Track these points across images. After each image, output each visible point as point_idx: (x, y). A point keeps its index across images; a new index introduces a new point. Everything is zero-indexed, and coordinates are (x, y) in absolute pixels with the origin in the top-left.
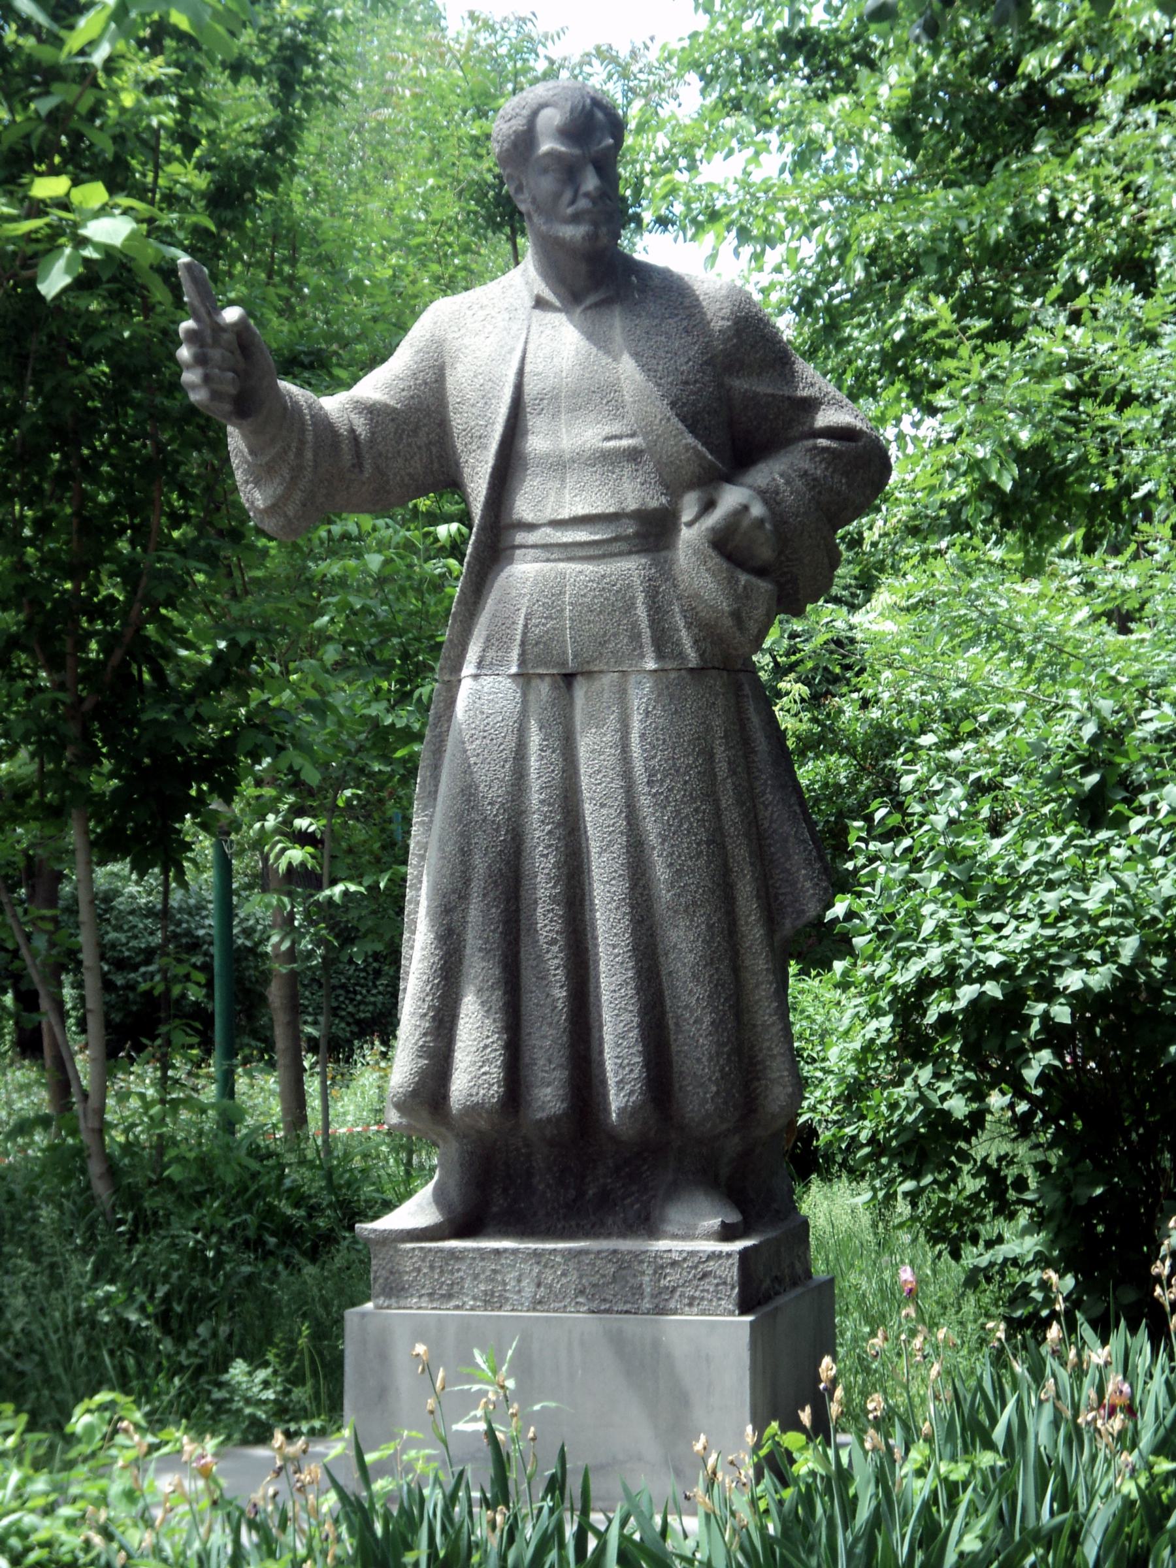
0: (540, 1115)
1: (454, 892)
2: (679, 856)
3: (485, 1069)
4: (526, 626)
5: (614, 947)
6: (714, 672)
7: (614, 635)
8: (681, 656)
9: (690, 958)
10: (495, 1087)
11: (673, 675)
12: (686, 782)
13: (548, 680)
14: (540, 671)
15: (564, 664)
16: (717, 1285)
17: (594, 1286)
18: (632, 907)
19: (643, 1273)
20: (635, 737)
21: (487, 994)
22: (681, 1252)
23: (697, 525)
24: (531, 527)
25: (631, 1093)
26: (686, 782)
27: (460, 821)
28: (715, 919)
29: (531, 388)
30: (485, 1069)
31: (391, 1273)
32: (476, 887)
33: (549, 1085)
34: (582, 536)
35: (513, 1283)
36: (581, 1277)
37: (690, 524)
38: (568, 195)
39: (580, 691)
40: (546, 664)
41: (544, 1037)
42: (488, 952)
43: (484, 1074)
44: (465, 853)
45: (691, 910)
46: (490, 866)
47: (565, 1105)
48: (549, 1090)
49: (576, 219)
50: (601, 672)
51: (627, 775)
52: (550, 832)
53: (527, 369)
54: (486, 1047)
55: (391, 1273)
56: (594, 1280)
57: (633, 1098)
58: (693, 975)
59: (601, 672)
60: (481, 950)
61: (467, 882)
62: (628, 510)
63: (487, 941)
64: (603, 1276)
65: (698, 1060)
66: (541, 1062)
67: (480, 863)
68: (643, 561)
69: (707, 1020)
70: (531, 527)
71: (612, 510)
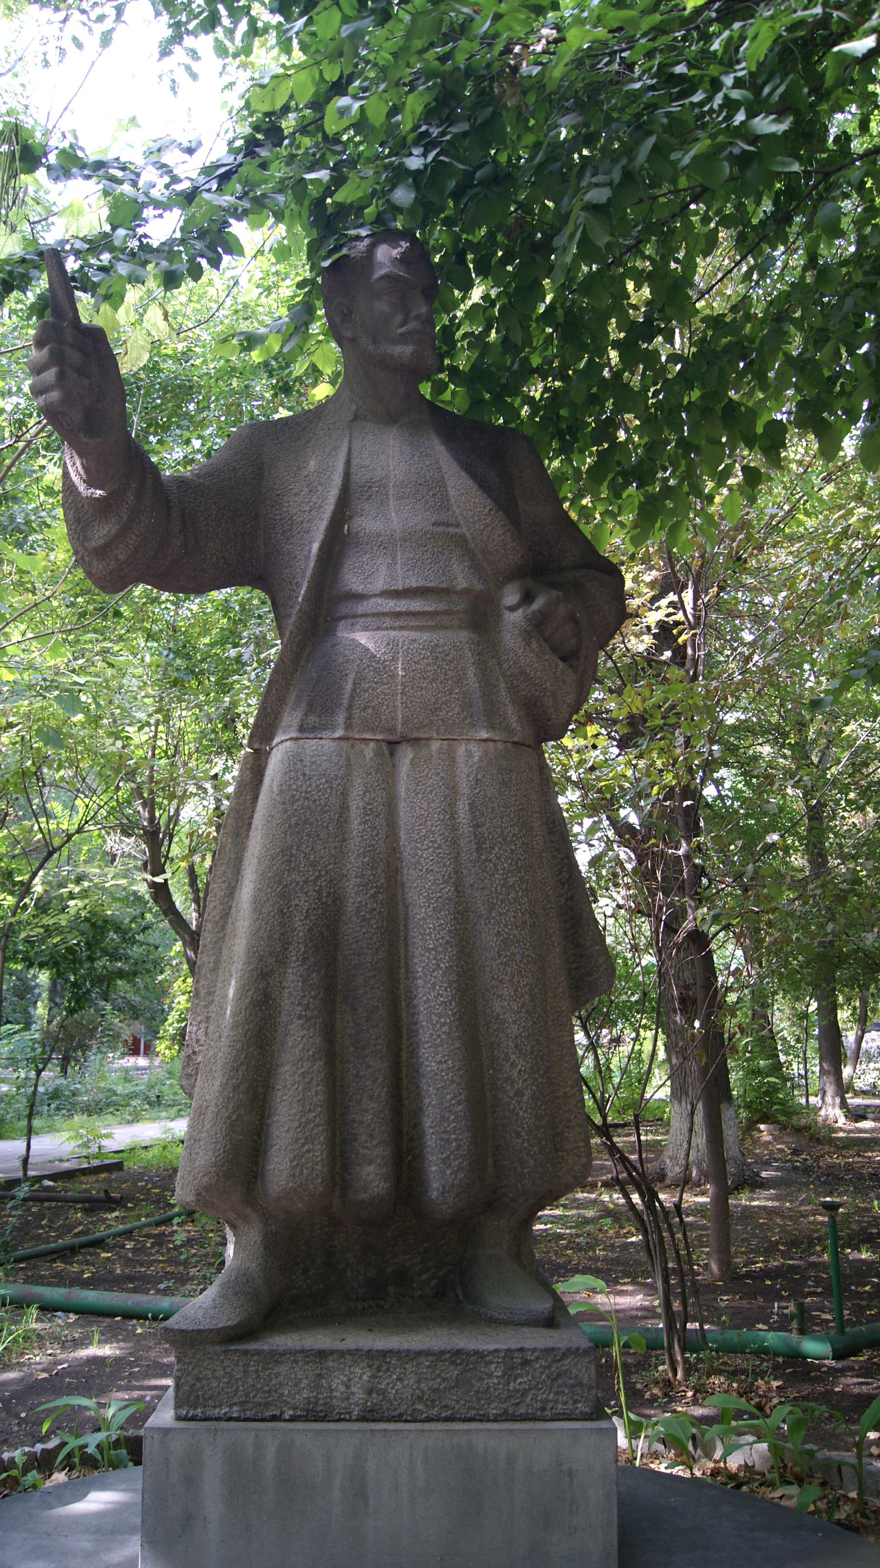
0: (363, 1196)
1: (271, 954)
2: (506, 926)
3: (306, 1148)
4: (354, 690)
5: (440, 1016)
6: (530, 750)
7: (446, 703)
8: (507, 729)
9: (514, 1029)
10: (319, 1167)
11: (500, 745)
12: (512, 851)
13: (372, 745)
14: (367, 736)
15: (391, 730)
16: (573, 1386)
17: (436, 1390)
18: (458, 975)
19: (490, 1376)
20: (462, 806)
21: (307, 1065)
22: (535, 1350)
23: (520, 610)
24: (361, 597)
25: (460, 1168)
26: (512, 851)
27: (280, 882)
28: (536, 990)
29: (358, 477)
30: (306, 1148)
31: (198, 1379)
32: (296, 951)
33: (370, 1164)
34: (416, 605)
35: (342, 1388)
36: (419, 1382)
37: (512, 609)
38: (399, 318)
39: (406, 756)
40: (373, 730)
41: (366, 1111)
42: (308, 1019)
43: (308, 1151)
44: (284, 915)
45: (516, 978)
46: (310, 930)
47: (387, 1185)
48: (371, 1168)
49: (404, 339)
50: (428, 739)
51: (455, 843)
52: (374, 896)
53: (354, 462)
54: (309, 1121)
55: (198, 1379)
56: (434, 1384)
57: (461, 1176)
58: (516, 1047)
59: (428, 739)
60: (300, 1017)
61: (286, 946)
62: (459, 588)
63: (307, 1008)
64: (445, 1380)
65: (518, 1135)
66: (363, 1138)
67: (299, 925)
68: (472, 636)
69: (528, 1093)
70: (361, 597)
71: (444, 585)
